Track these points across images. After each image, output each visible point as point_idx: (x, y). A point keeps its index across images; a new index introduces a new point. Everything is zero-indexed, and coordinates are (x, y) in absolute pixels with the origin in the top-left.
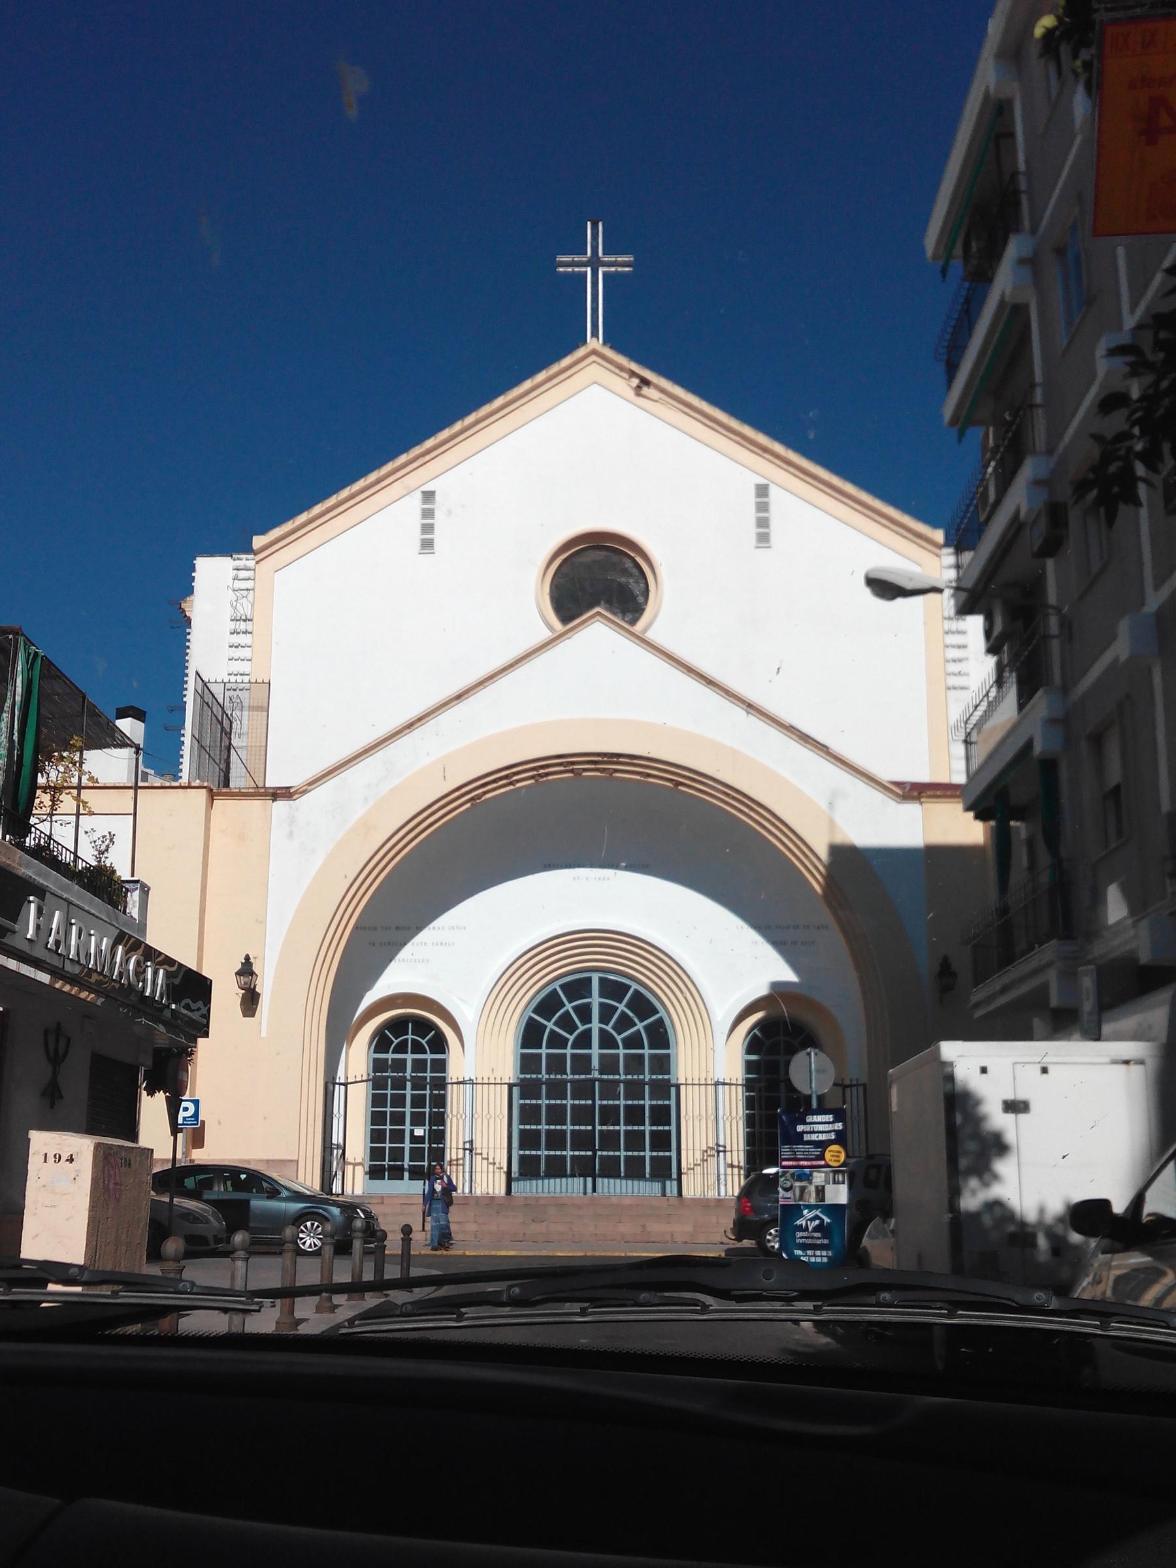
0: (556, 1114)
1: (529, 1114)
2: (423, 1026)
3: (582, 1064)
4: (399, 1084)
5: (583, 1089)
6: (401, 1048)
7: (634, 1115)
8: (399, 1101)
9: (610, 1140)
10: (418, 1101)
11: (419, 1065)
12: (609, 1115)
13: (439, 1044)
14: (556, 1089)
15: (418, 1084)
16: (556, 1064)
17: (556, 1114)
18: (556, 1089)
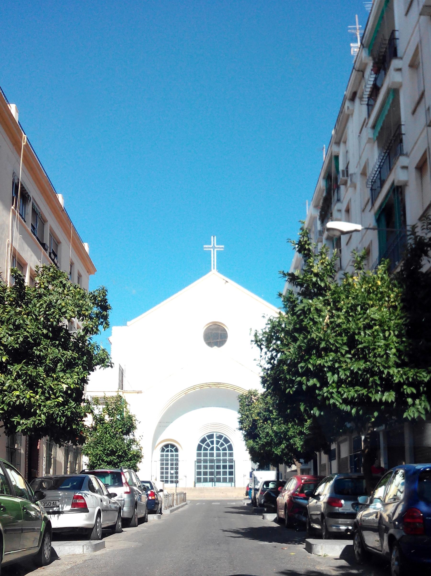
0: (205, 467)
1: (199, 467)
2: (173, 446)
3: (212, 455)
4: (167, 460)
5: (212, 461)
6: (168, 451)
7: (224, 467)
8: (167, 464)
9: (219, 473)
10: (172, 464)
11: (172, 456)
12: (218, 467)
13: (176, 450)
14: (205, 461)
15: (172, 460)
16: (205, 455)
17: (205, 467)
18: (205, 461)
